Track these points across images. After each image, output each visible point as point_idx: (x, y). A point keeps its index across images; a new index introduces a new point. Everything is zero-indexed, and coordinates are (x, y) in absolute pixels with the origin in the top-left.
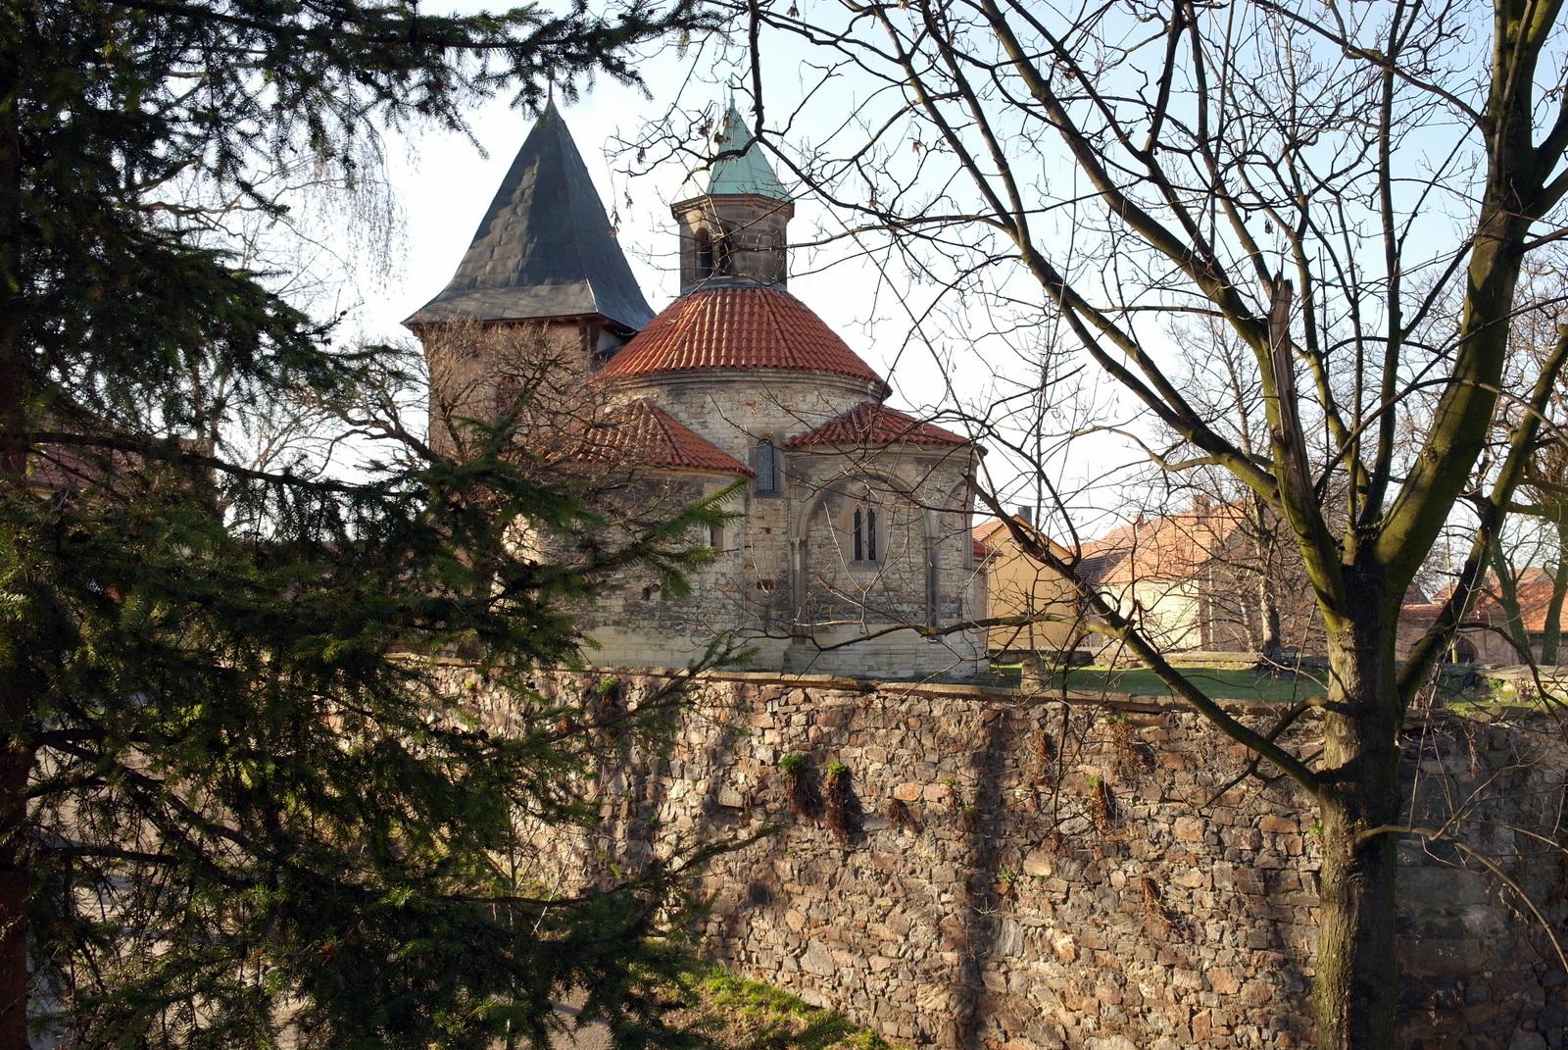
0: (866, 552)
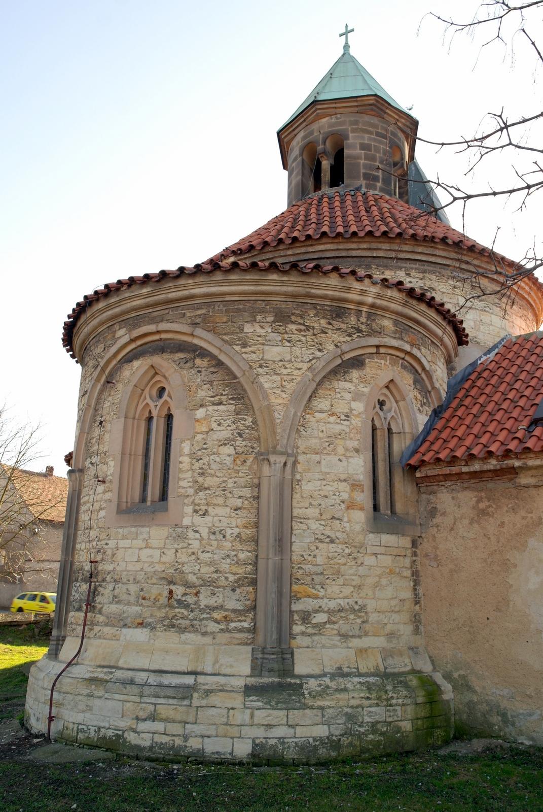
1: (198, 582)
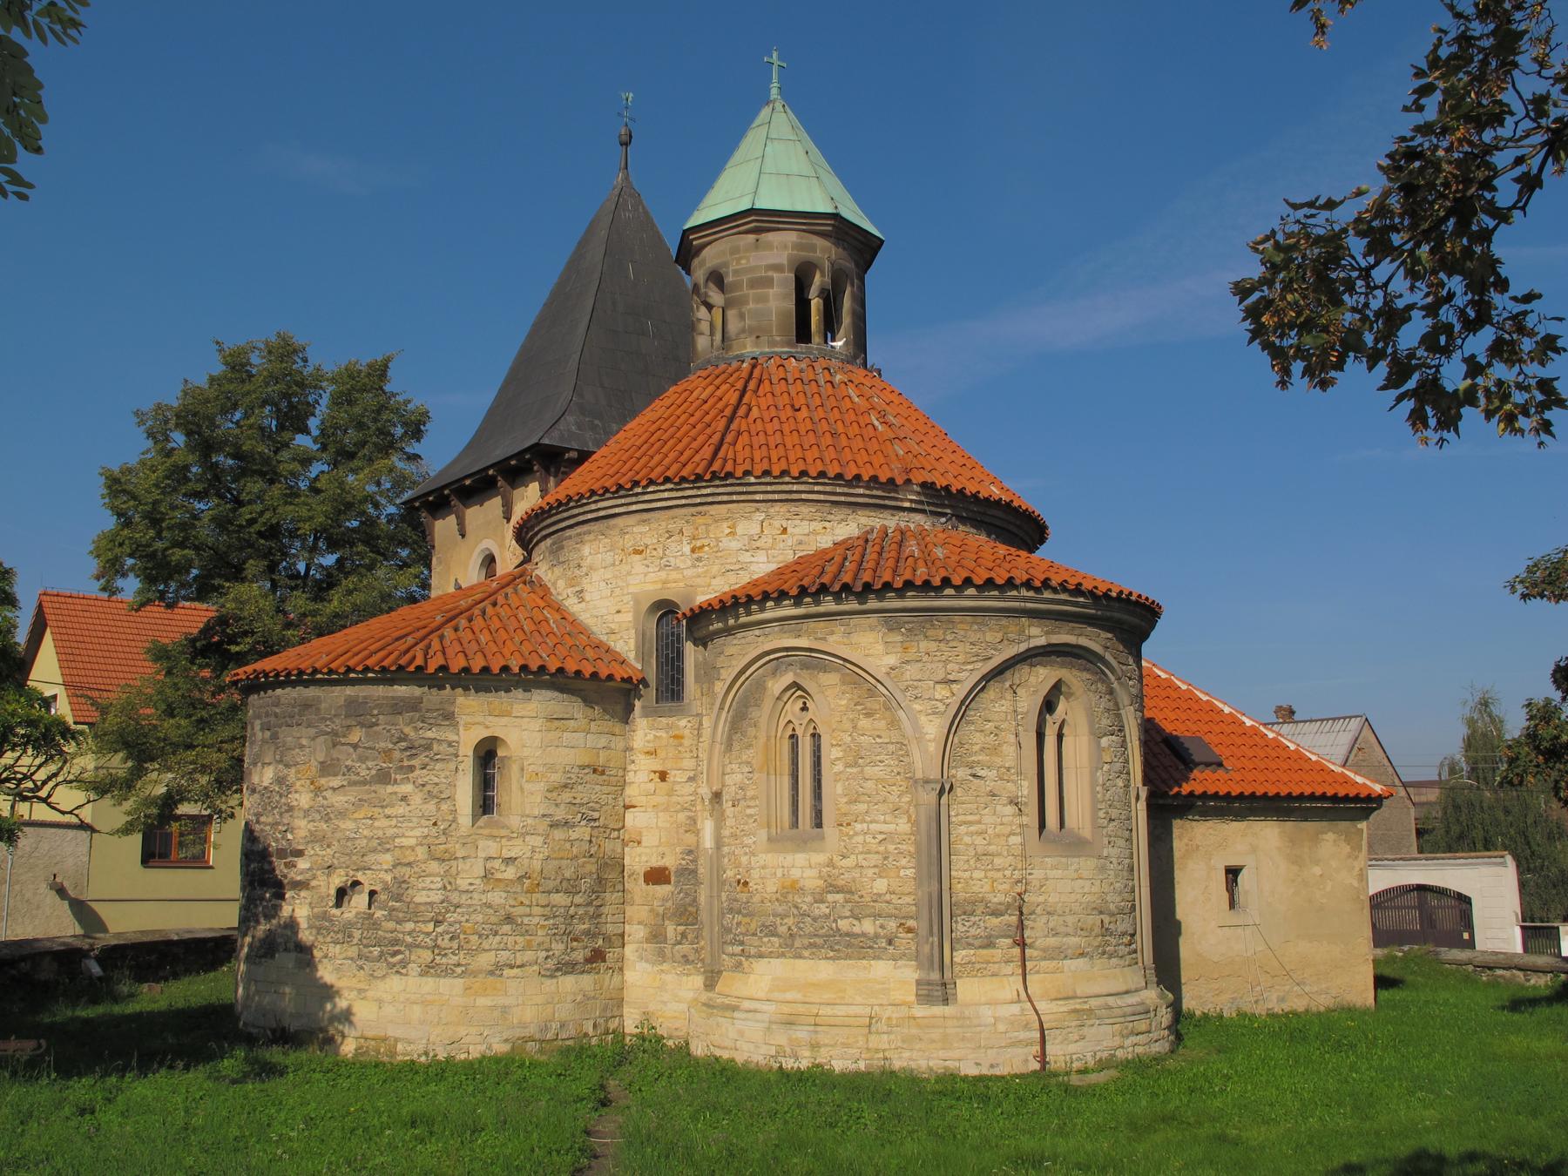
0: (808, 812)
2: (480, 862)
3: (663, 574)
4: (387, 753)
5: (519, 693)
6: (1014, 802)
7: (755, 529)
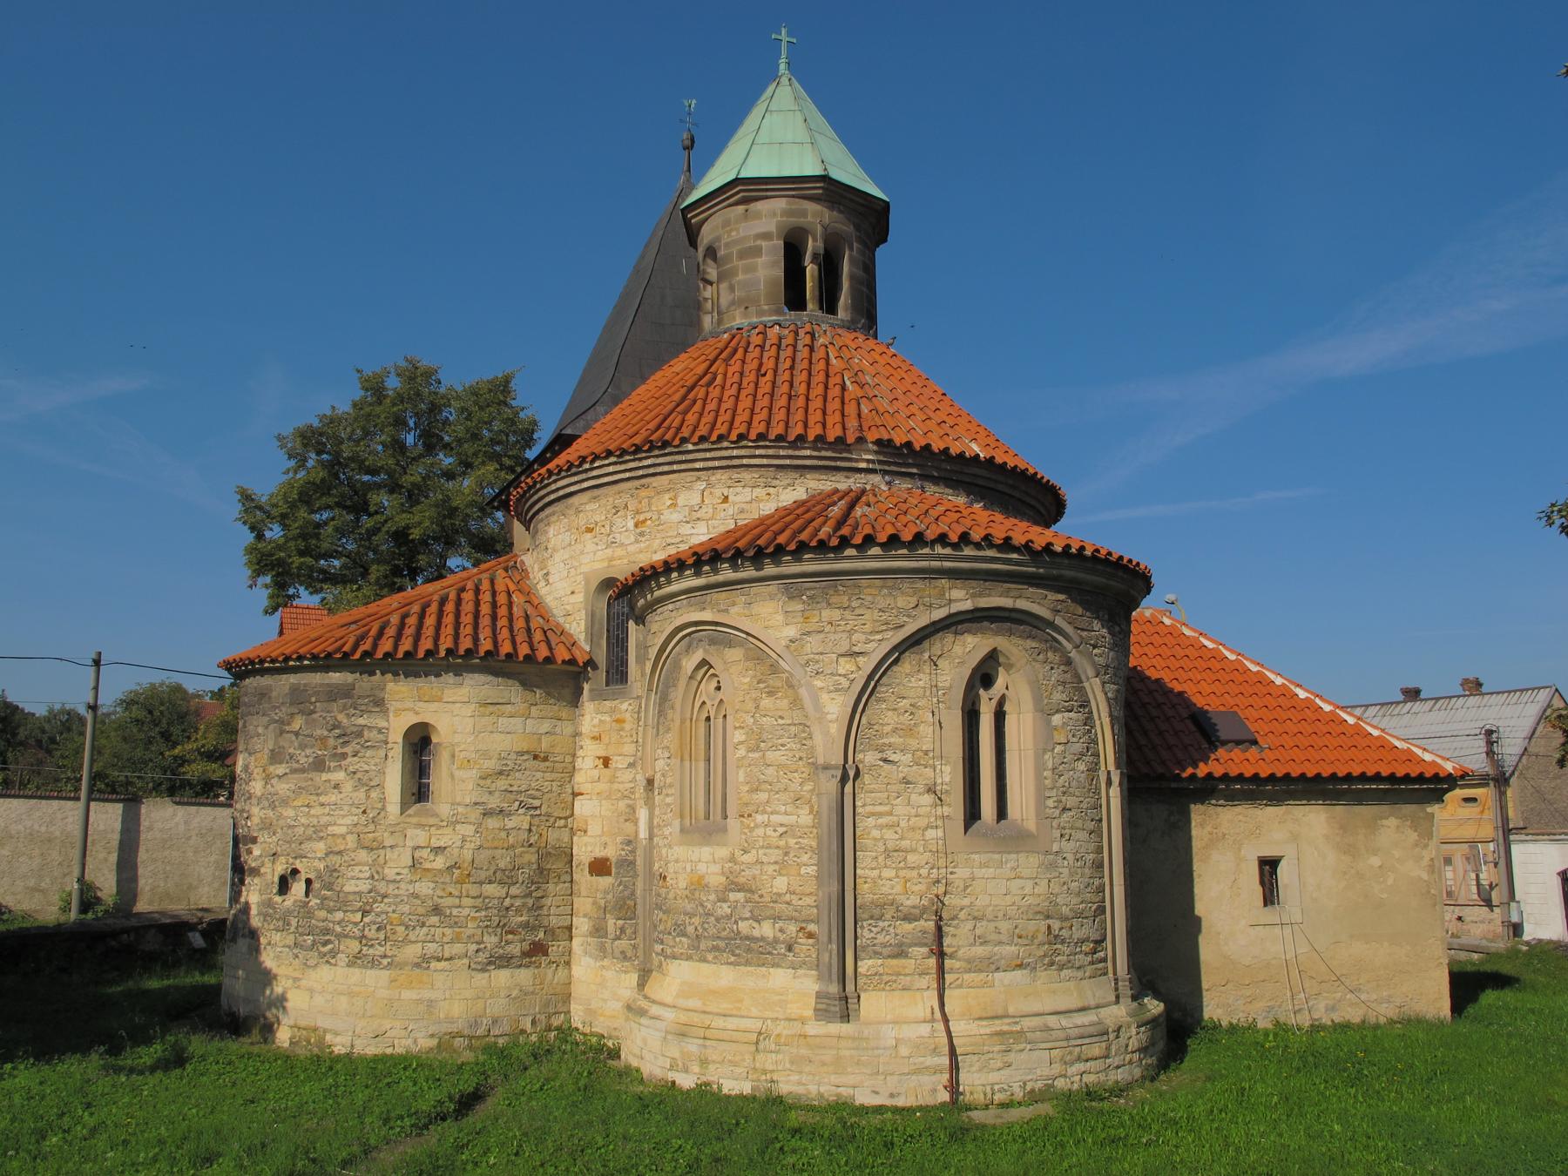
1: (1071, 915)
2: (409, 853)
3: (609, 551)
4: (323, 739)
5: (449, 678)
6: (931, 790)
7: (696, 499)
